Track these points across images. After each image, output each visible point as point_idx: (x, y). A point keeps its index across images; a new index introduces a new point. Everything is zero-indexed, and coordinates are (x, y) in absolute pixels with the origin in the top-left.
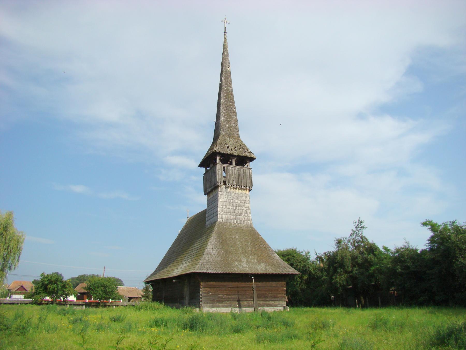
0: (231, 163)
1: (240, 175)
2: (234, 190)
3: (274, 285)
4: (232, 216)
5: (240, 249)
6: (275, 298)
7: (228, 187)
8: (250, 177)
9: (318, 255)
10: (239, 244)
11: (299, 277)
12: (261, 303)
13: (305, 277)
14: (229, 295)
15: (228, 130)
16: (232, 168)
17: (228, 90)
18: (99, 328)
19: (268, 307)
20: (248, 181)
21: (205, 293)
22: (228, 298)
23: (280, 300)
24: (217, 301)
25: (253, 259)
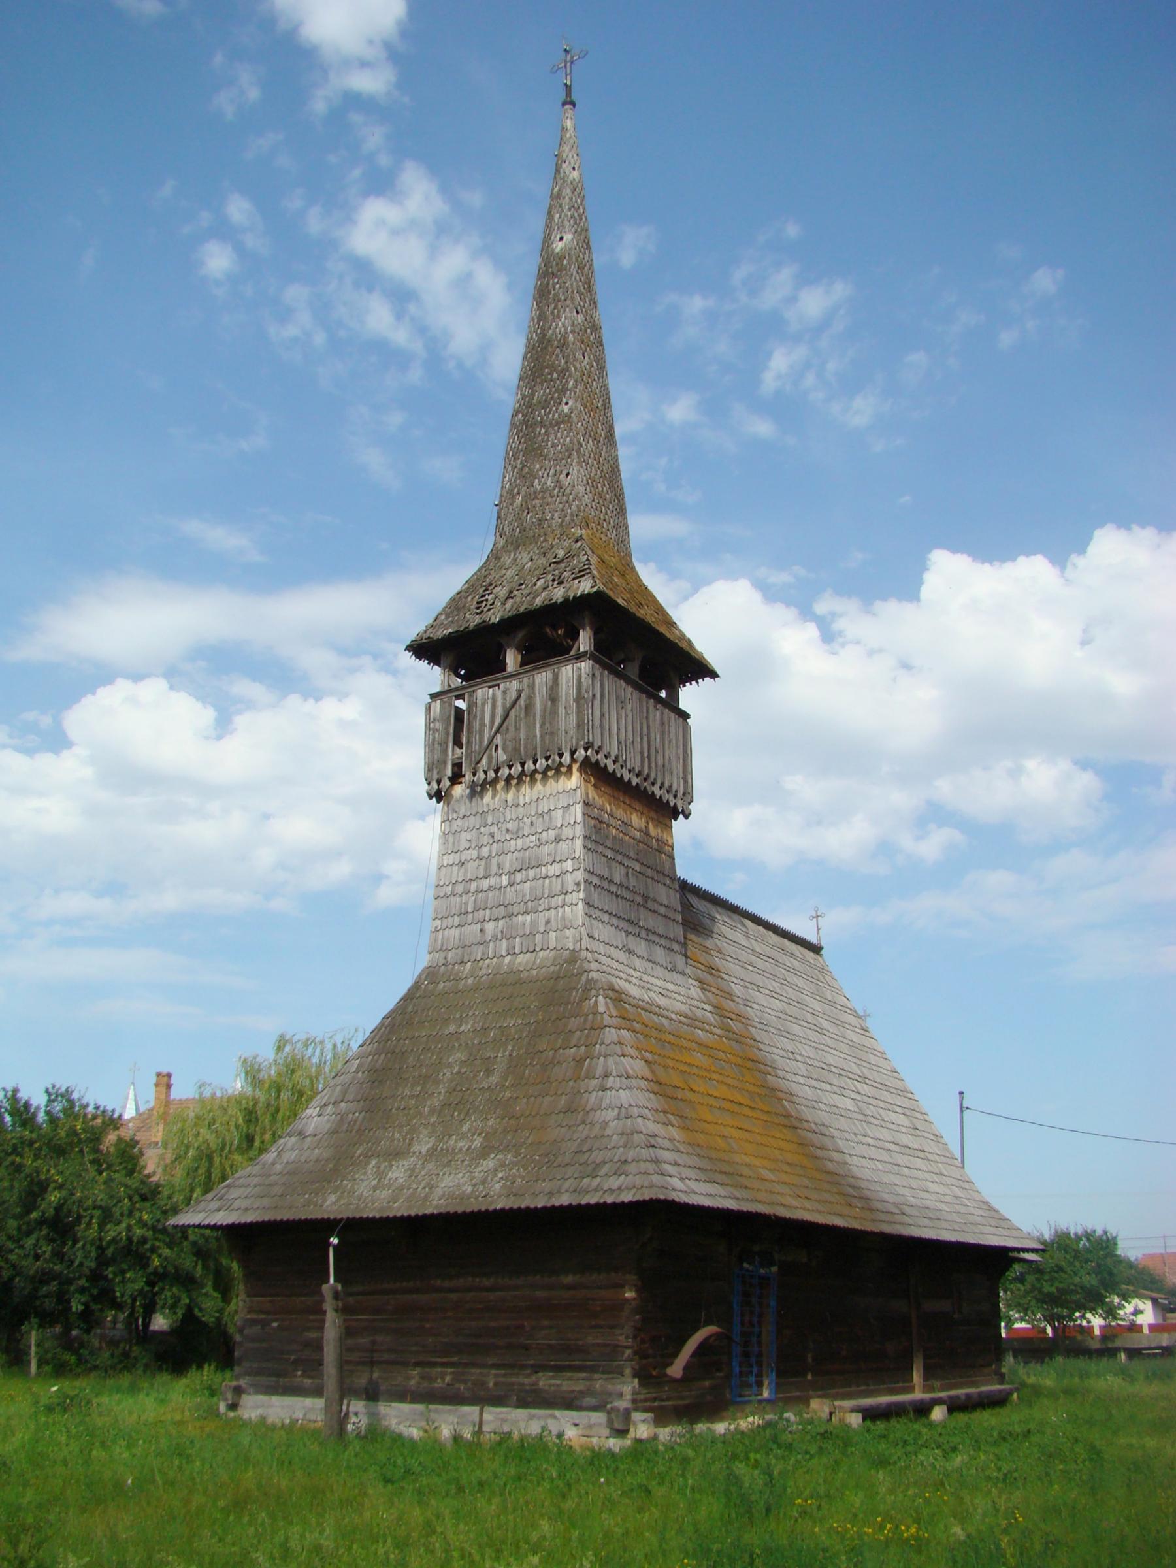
0: (503, 668)
4: (490, 927)
6: (569, 1357)
19: (523, 1404)
23: (593, 1369)
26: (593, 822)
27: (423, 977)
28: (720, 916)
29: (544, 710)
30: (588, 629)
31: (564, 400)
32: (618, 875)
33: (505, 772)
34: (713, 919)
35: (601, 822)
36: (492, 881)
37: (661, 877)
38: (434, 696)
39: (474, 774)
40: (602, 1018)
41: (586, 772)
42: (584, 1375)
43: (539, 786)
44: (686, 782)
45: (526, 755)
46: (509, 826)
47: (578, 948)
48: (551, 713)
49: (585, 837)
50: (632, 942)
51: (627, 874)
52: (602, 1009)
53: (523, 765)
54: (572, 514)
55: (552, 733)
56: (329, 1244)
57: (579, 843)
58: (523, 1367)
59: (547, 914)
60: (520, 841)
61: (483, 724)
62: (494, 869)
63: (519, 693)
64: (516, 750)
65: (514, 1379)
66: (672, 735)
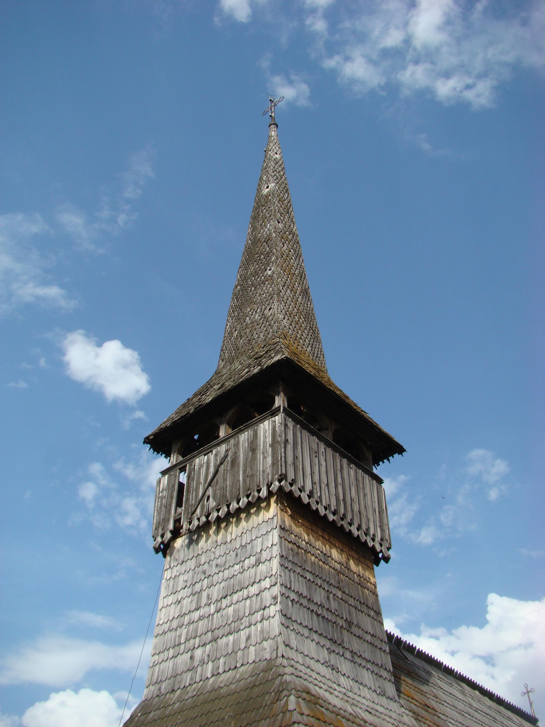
26: (290, 545)
27: (138, 711)
28: (435, 673)
29: (246, 460)
30: (282, 394)
31: (268, 268)
32: (319, 596)
33: (214, 515)
34: (430, 674)
35: (299, 547)
36: (202, 611)
37: (364, 608)
38: (164, 473)
40: (291, 716)
41: (282, 504)
43: (243, 523)
44: (382, 530)
45: (231, 498)
46: (219, 561)
47: (274, 657)
48: (252, 460)
49: (282, 556)
50: (334, 659)
51: (328, 598)
52: (291, 707)
53: (228, 506)
54: (273, 332)
55: (252, 475)
57: (275, 563)
59: (247, 630)
61: (198, 483)
62: (204, 600)
63: (227, 451)
64: (224, 496)
66: (368, 491)
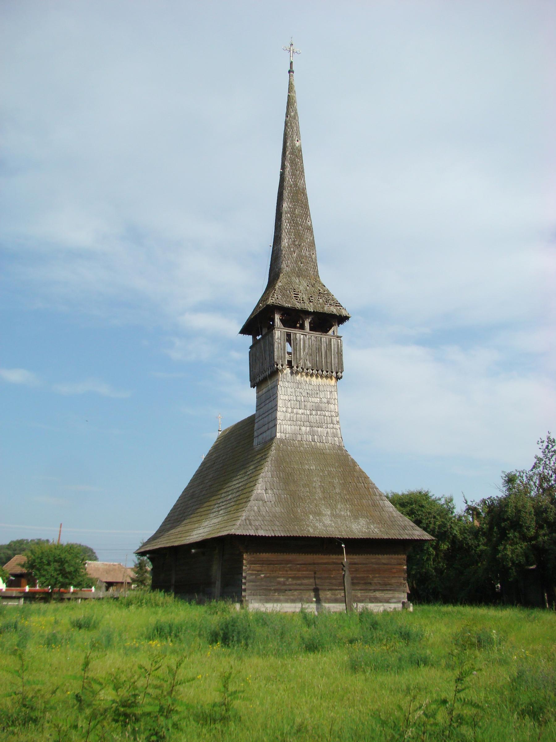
0: (302, 327)
1: (319, 349)
2: (308, 379)
3: (383, 561)
4: (303, 428)
5: (318, 490)
6: (385, 586)
7: (297, 373)
8: (338, 353)
9: (469, 503)
10: (317, 482)
11: (432, 546)
12: (359, 595)
13: (444, 546)
14: (298, 578)
15: (296, 262)
16: (305, 337)
17: (296, 185)
18: (51, 641)
19: (371, 602)
20: (335, 361)
21: (252, 574)
22: (296, 584)
23: (394, 590)
24: (275, 590)
25: (344, 510)
39: (297, 367)
42: (391, 592)
56: (342, 548)
58: (370, 590)
60: (313, 399)
65: (367, 594)
